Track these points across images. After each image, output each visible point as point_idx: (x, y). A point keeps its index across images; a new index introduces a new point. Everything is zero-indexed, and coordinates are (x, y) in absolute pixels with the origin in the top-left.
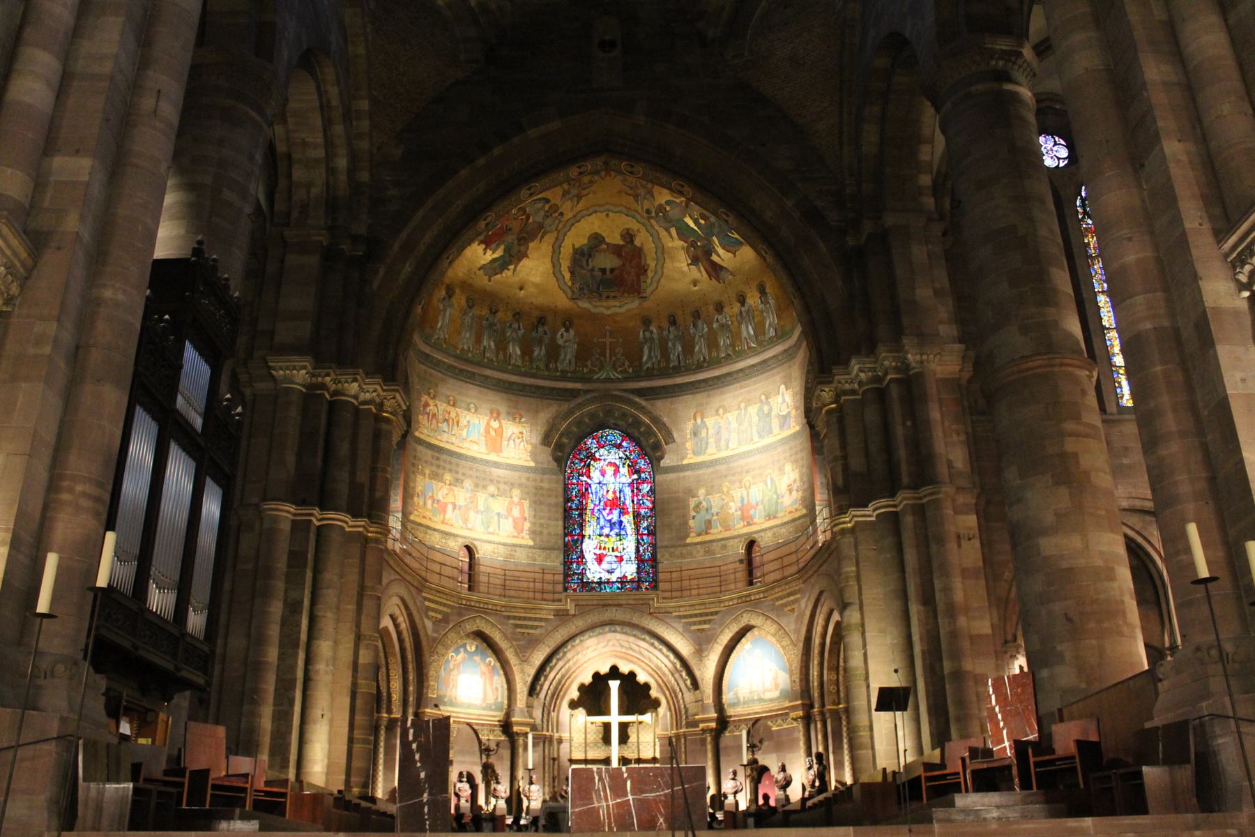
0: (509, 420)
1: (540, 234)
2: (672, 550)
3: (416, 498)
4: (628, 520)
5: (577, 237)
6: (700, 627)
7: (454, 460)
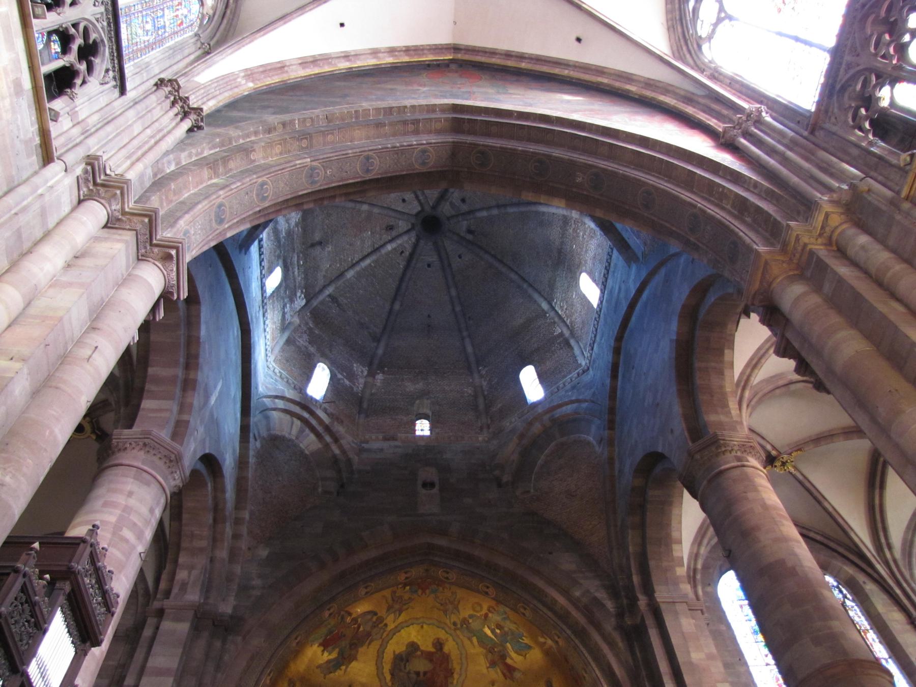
1: (368, 641)
5: (396, 646)
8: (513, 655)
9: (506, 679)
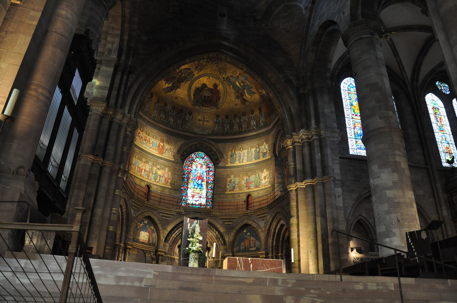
0: (167, 143)
1: (185, 81)
2: (220, 195)
3: (132, 165)
4: (204, 184)
5: (197, 84)
6: (228, 223)
7: (147, 154)
8: (247, 95)
9: (242, 104)
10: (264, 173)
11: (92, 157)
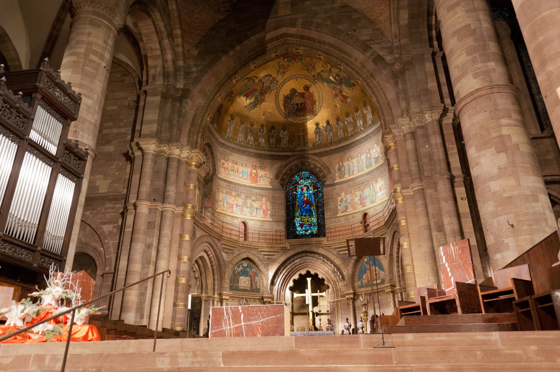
3: (219, 203)
4: (313, 208)
5: (285, 90)
7: (236, 186)
10: (378, 184)
11: (148, 203)
